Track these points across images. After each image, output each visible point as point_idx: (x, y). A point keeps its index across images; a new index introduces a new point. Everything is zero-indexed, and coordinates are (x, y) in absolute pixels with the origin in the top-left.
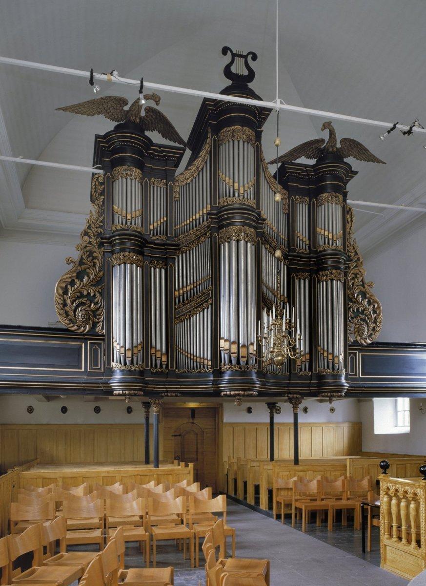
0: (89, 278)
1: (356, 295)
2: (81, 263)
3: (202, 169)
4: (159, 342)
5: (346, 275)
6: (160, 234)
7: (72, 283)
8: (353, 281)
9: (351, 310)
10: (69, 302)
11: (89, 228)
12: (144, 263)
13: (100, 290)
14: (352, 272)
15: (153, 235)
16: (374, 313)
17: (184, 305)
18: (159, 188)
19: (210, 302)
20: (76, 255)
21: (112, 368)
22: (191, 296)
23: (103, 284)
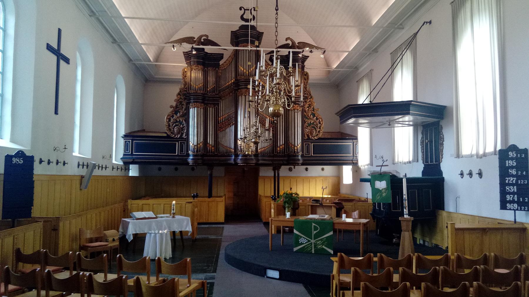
4: (211, 141)
7: (173, 116)
10: (171, 124)
11: (180, 92)
20: (174, 104)
23: (186, 116)
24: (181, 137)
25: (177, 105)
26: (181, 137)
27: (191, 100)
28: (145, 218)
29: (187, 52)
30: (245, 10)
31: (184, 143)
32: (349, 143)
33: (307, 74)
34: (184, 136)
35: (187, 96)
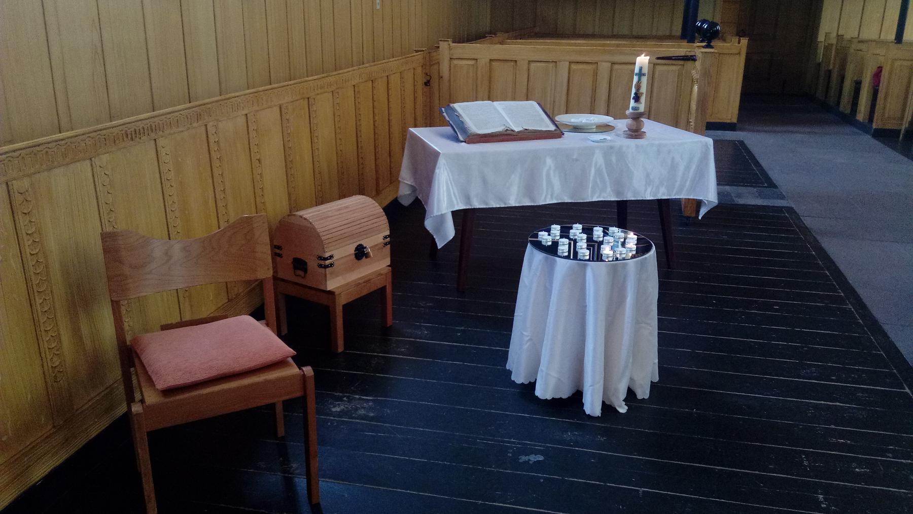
28: (507, 136)
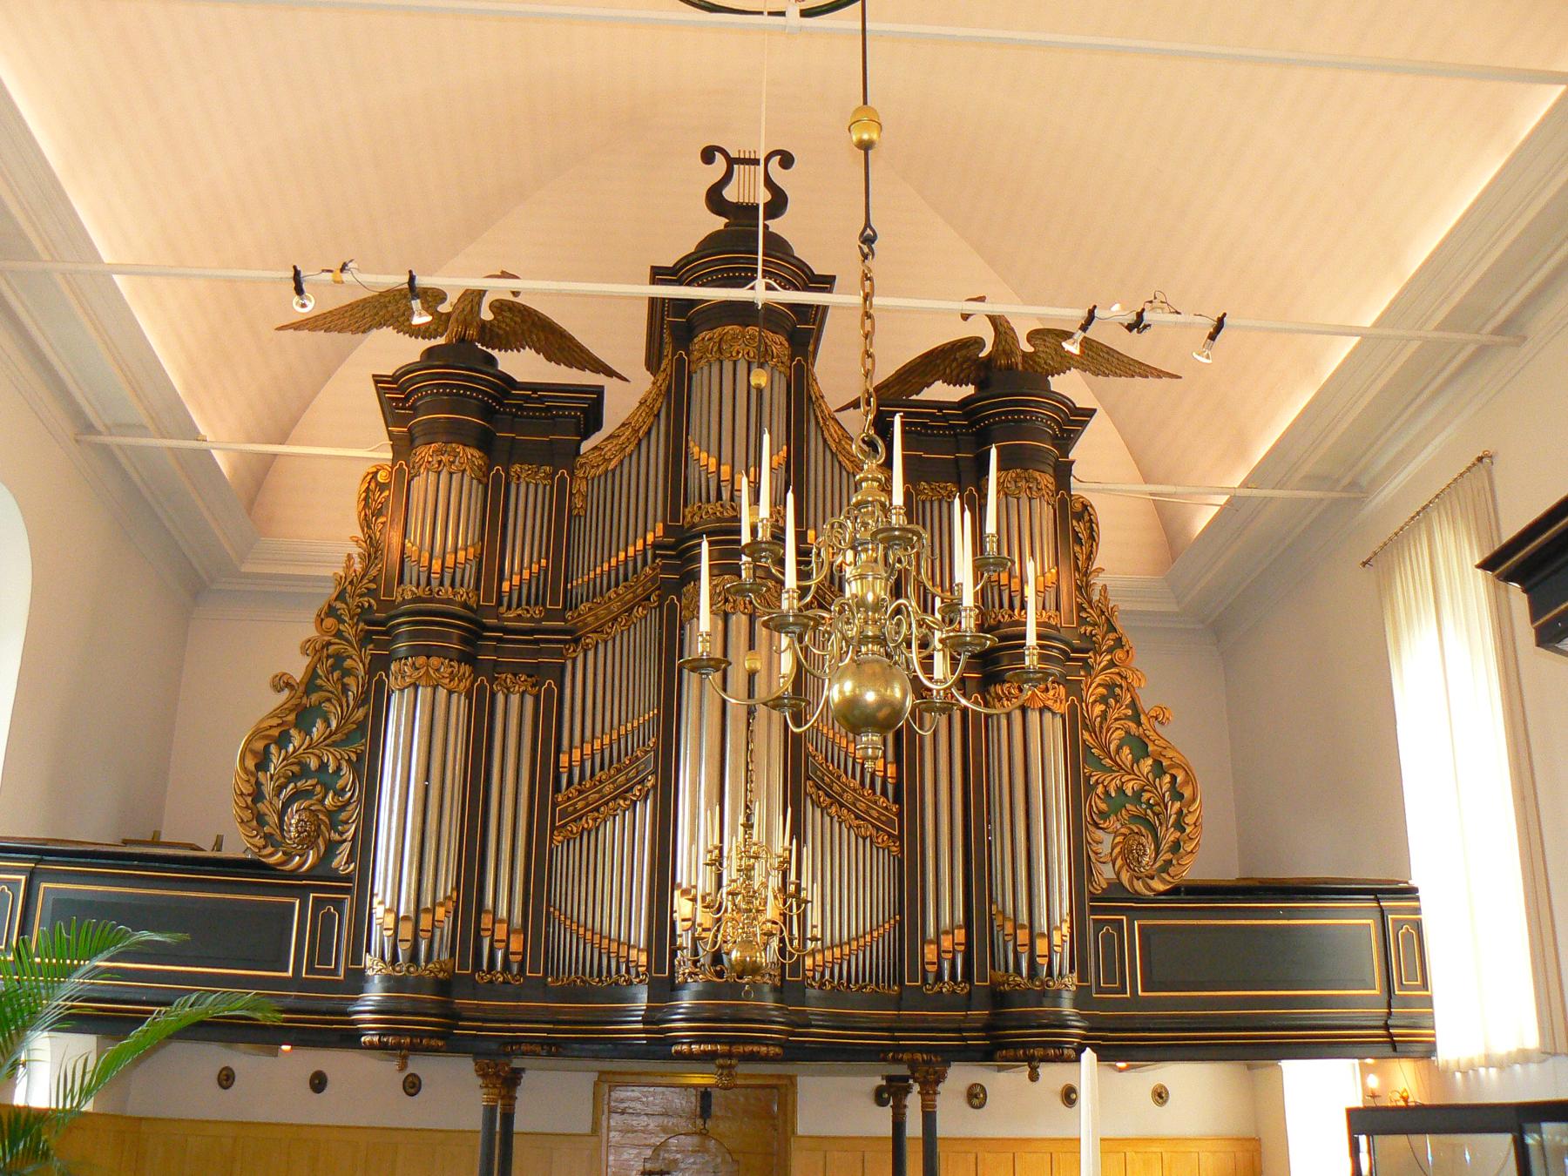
0: (329, 726)
1: (1113, 747)
2: (311, 684)
3: (648, 433)
4: (504, 896)
5: (1074, 688)
6: (528, 603)
7: (283, 740)
8: (1103, 707)
9: (1100, 789)
10: (268, 788)
11: (341, 596)
12: (475, 680)
13: (354, 758)
14: (1098, 680)
15: (509, 607)
16: (1173, 800)
17: (580, 792)
18: (532, 487)
19: (649, 784)
20: (297, 668)
21: (363, 971)
22: (602, 768)
24: (323, 871)
25: (312, 674)
26: (323, 871)
27: (395, 639)
29: (394, 378)
30: (732, 162)
31: (338, 904)
32: (1357, 919)
33: (1085, 512)
34: (340, 862)
35: (376, 625)
